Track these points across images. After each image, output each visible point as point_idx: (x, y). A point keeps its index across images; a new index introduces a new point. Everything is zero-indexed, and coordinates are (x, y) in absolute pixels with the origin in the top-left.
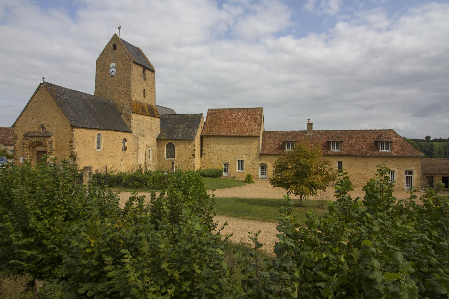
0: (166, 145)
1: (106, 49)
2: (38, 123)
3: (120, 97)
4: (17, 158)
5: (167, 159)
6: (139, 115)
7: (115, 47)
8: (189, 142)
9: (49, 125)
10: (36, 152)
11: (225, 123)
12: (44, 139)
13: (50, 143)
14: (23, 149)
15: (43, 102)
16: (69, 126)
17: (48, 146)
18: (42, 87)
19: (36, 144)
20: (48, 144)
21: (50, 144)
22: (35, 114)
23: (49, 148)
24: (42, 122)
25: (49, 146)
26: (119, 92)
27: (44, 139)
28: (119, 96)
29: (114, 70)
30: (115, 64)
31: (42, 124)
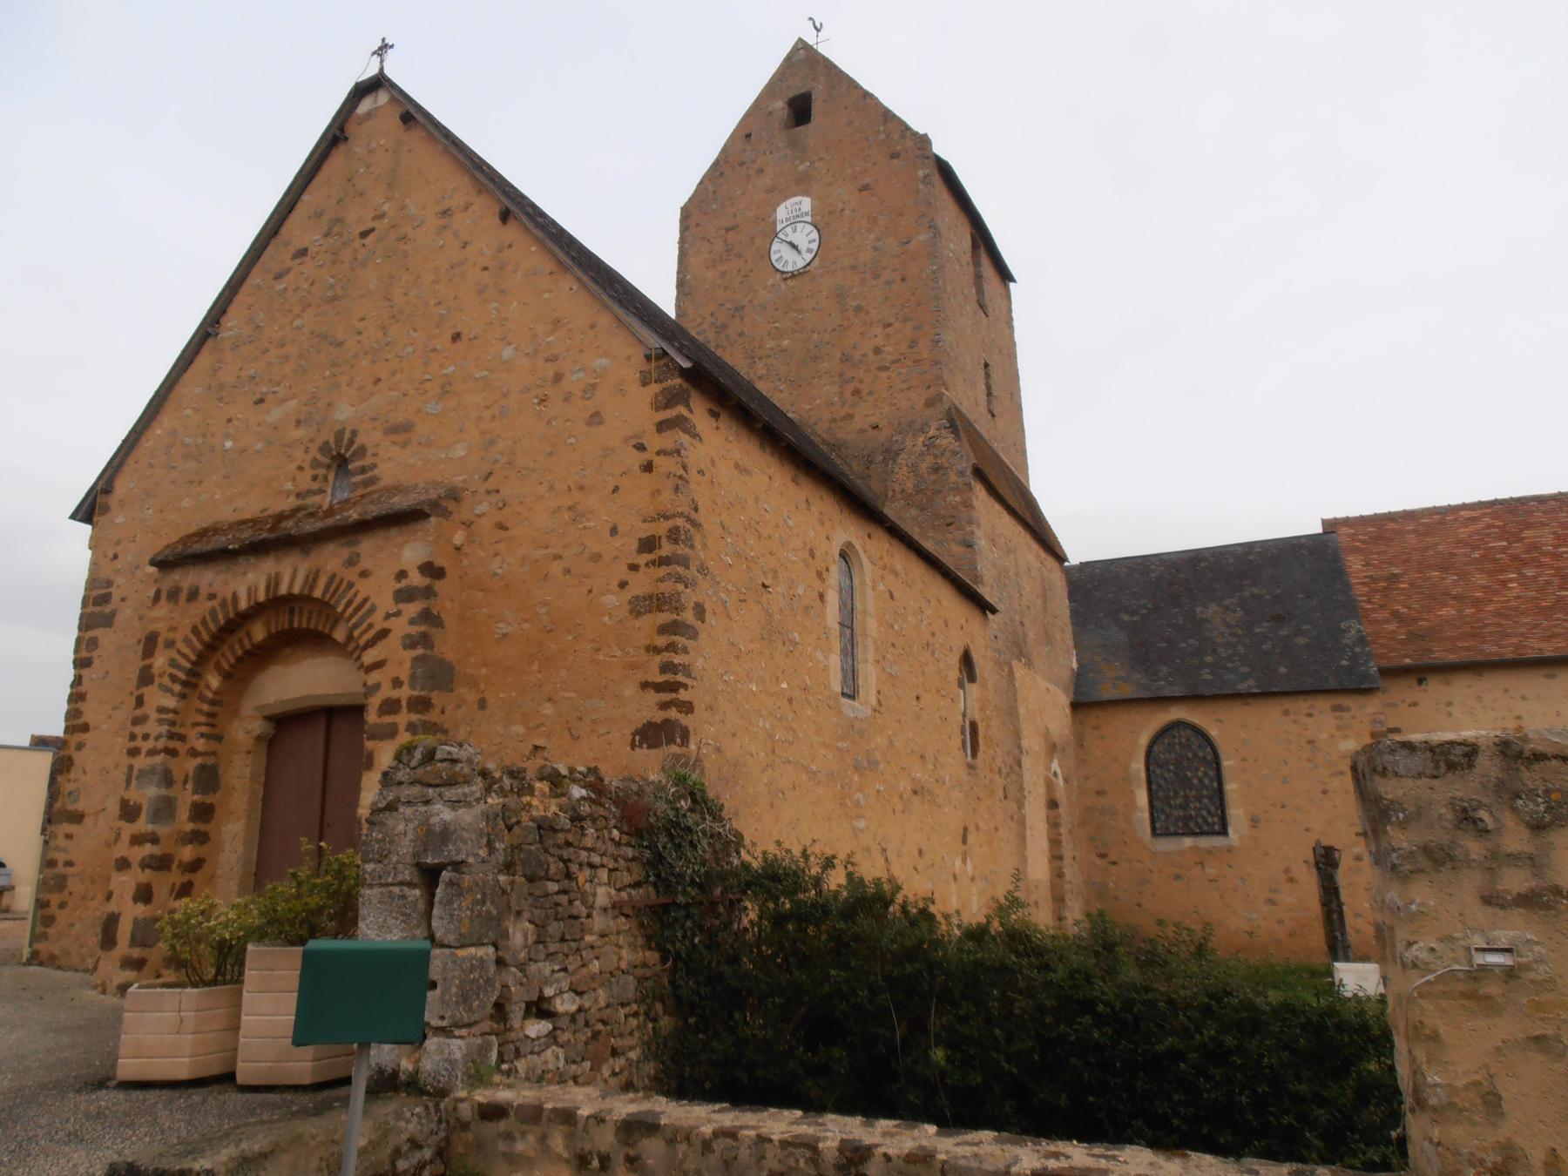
0: (1144, 740)
1: (745, 133)
2: (300, 433)
3: (857, 392)
4: (80, 806)
5: (1166, 845)
6: (997, 507)
7: (800, 110)
8: (1337, 708)
9: (406, 428)
10: (258, 727)
11: (1504, 583)
12: (351, 562)
13: (405, 596)
14: (140, 702)
15: (364, 234)
16: (634, 388)
17: (384, 634)
18: (369, 115)
19: (259, 632)
20: (385, 603)
21: (412, 609)
22: (287, 358)
23: (389, 649)
24: (344, 413)
25: (401, 627)
26: (846, 359)
27: (351, 562)
28: (850, 388)
29: (806, 237)
30: (806, 203)
31: (339, 435)
